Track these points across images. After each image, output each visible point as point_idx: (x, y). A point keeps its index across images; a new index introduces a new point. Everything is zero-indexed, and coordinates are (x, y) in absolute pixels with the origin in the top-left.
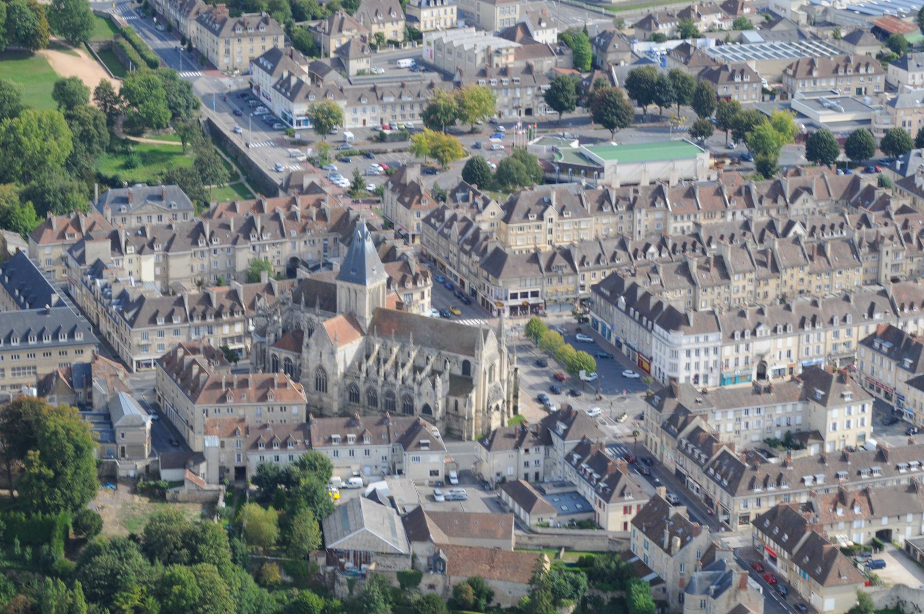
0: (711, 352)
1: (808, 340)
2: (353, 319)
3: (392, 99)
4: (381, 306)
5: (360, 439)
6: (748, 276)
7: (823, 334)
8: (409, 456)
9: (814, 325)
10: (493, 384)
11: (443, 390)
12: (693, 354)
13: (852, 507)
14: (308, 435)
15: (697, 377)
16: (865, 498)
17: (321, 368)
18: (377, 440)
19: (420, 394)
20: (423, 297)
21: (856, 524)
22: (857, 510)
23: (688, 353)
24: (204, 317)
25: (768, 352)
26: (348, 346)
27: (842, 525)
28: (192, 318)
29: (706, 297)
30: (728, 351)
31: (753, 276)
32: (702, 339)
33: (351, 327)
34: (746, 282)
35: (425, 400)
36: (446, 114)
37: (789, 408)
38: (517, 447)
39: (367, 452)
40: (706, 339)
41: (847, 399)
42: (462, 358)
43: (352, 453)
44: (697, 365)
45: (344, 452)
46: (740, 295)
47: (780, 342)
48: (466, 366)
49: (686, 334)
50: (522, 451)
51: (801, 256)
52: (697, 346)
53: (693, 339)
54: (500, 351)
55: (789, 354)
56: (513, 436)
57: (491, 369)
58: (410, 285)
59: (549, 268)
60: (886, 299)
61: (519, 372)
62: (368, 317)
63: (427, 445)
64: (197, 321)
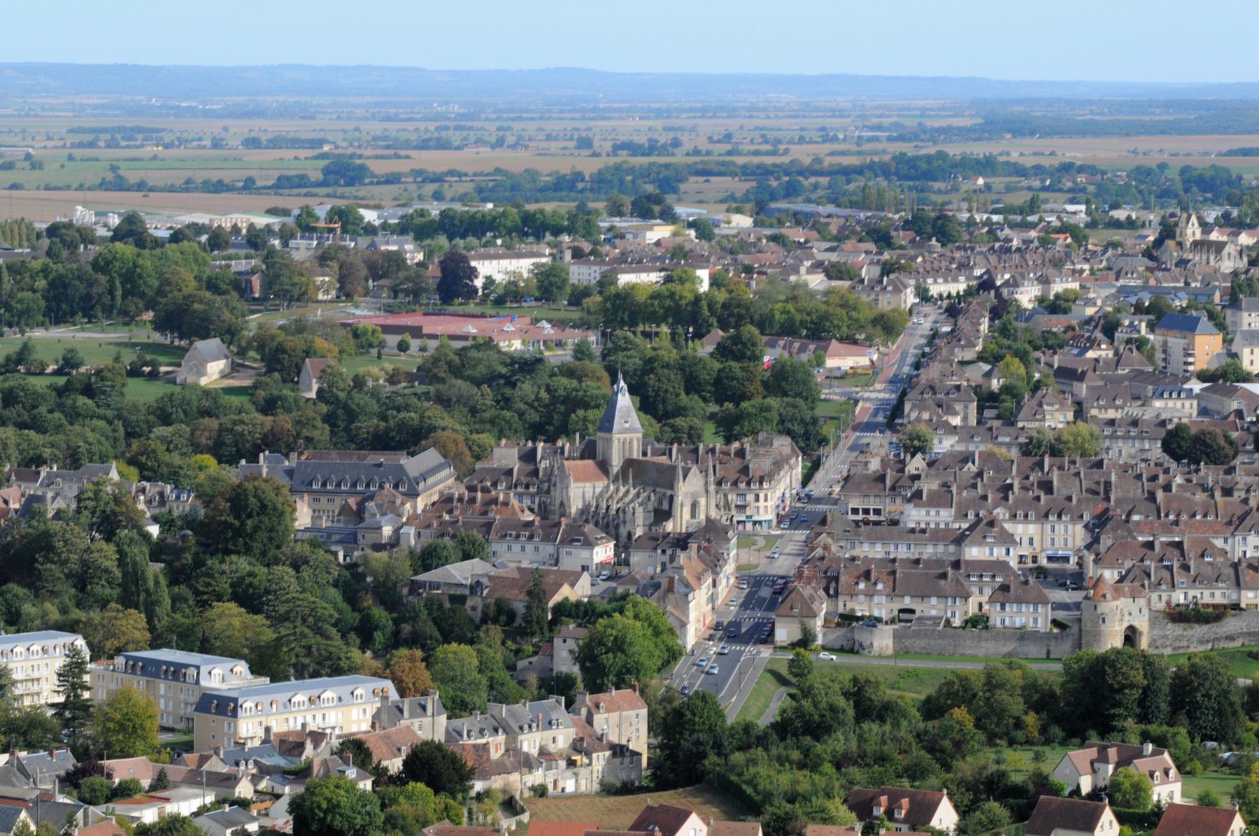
1: (1053, 530)
2: (604, 466)
3: (1007, 440)
4: (635, 456)
5: (531, 537)
7: (1070, 527)
8: (563, 551)
9: (1059, 516)
11: (645, 519)
13: (875, 584)
14: (488, 532)
16: (891, 578)
17: (562, 504)
18: (547, 538)
19: (624, 522)
20: (757, 500)
21: (876, 599)
22: (880, 586)
24: (527, 487)
26: (588, 484)
27: (861, 597)
28: (516, 487)
32: (933, 512)
33: (597, 471)
35: (628, 527)
36: (1039, 447)
37: (941, 548)
38: (655, 549)
39: (537, 549)
40: (938, 513)
41: (989, 540)
42: (669, 492)
43: (523, 549)
45: (516, 547)
48: (671, 498)
50: (659, 551)
51: (1140, 490)
53: (923, 512)
54: (707, 491)
55: (1031, 541)
56: (657, 539)
57: (694, 506)
58: (743, 485)
59: (893, 488)
60: (1153, 506)
62: (616, 464)
63: (579, 541)
64: (519, 490)
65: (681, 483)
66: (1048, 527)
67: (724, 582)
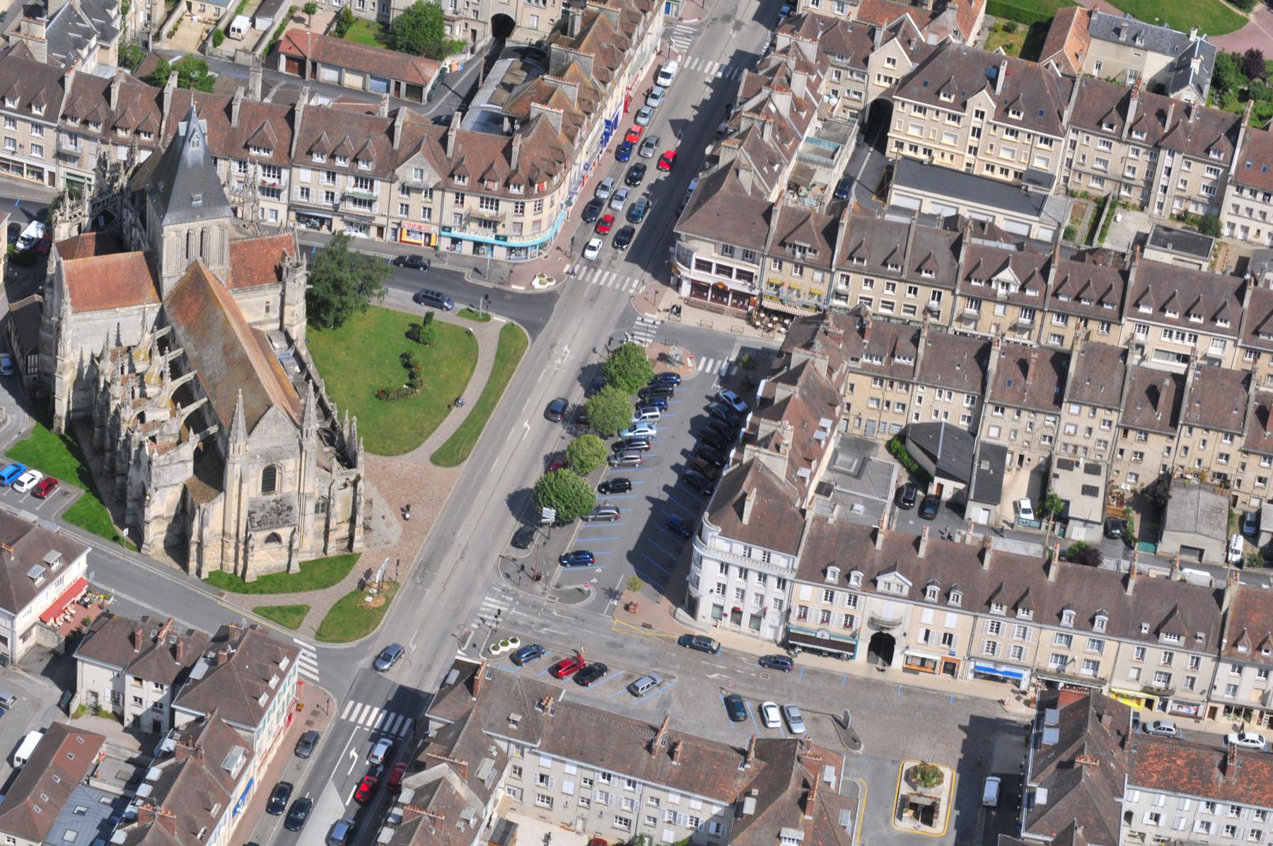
0: (772, 582)
6: (1100, 412)
10: (272, 497)
12: (734, 571)
15: (736, 612)
23: (725, 567)
25: (896, 624)
29: (999, 422)
30: (807, 593)
31: (1114, 417)
34: (1095, 424)
44: (742, 593)
46: (1079, 440)
47: (928, 615)
49: (724, 534)
52: (746, 564)
53: (739, 547)
55: (948, 639)
61: (360, 484)
65: (241, 443)
66: (985, 622)
67: (289, 689)
